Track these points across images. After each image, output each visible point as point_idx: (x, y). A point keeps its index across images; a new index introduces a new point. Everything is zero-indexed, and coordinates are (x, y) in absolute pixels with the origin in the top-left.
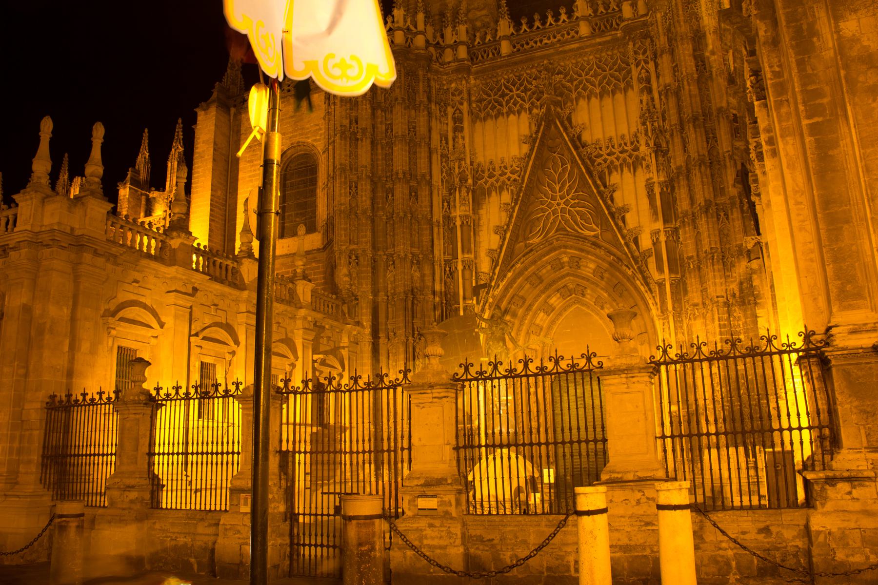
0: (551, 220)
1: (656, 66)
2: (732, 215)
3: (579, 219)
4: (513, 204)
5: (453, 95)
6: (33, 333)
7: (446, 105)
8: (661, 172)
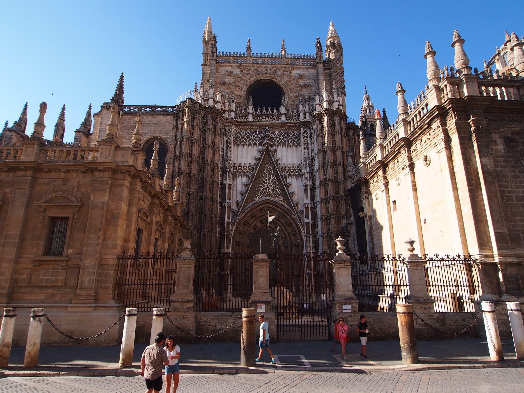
0: (264, 192)
4: (249, 183)
6: (108, 218)
7: (224, 136)
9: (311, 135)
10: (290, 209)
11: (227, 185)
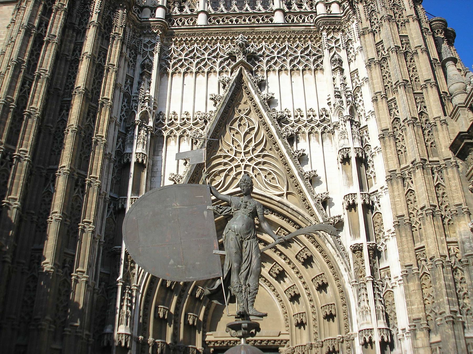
0: (233, 174)
2: (447, 174)
5: (145, 46)
9: (347, 43)
10: (307, 216)
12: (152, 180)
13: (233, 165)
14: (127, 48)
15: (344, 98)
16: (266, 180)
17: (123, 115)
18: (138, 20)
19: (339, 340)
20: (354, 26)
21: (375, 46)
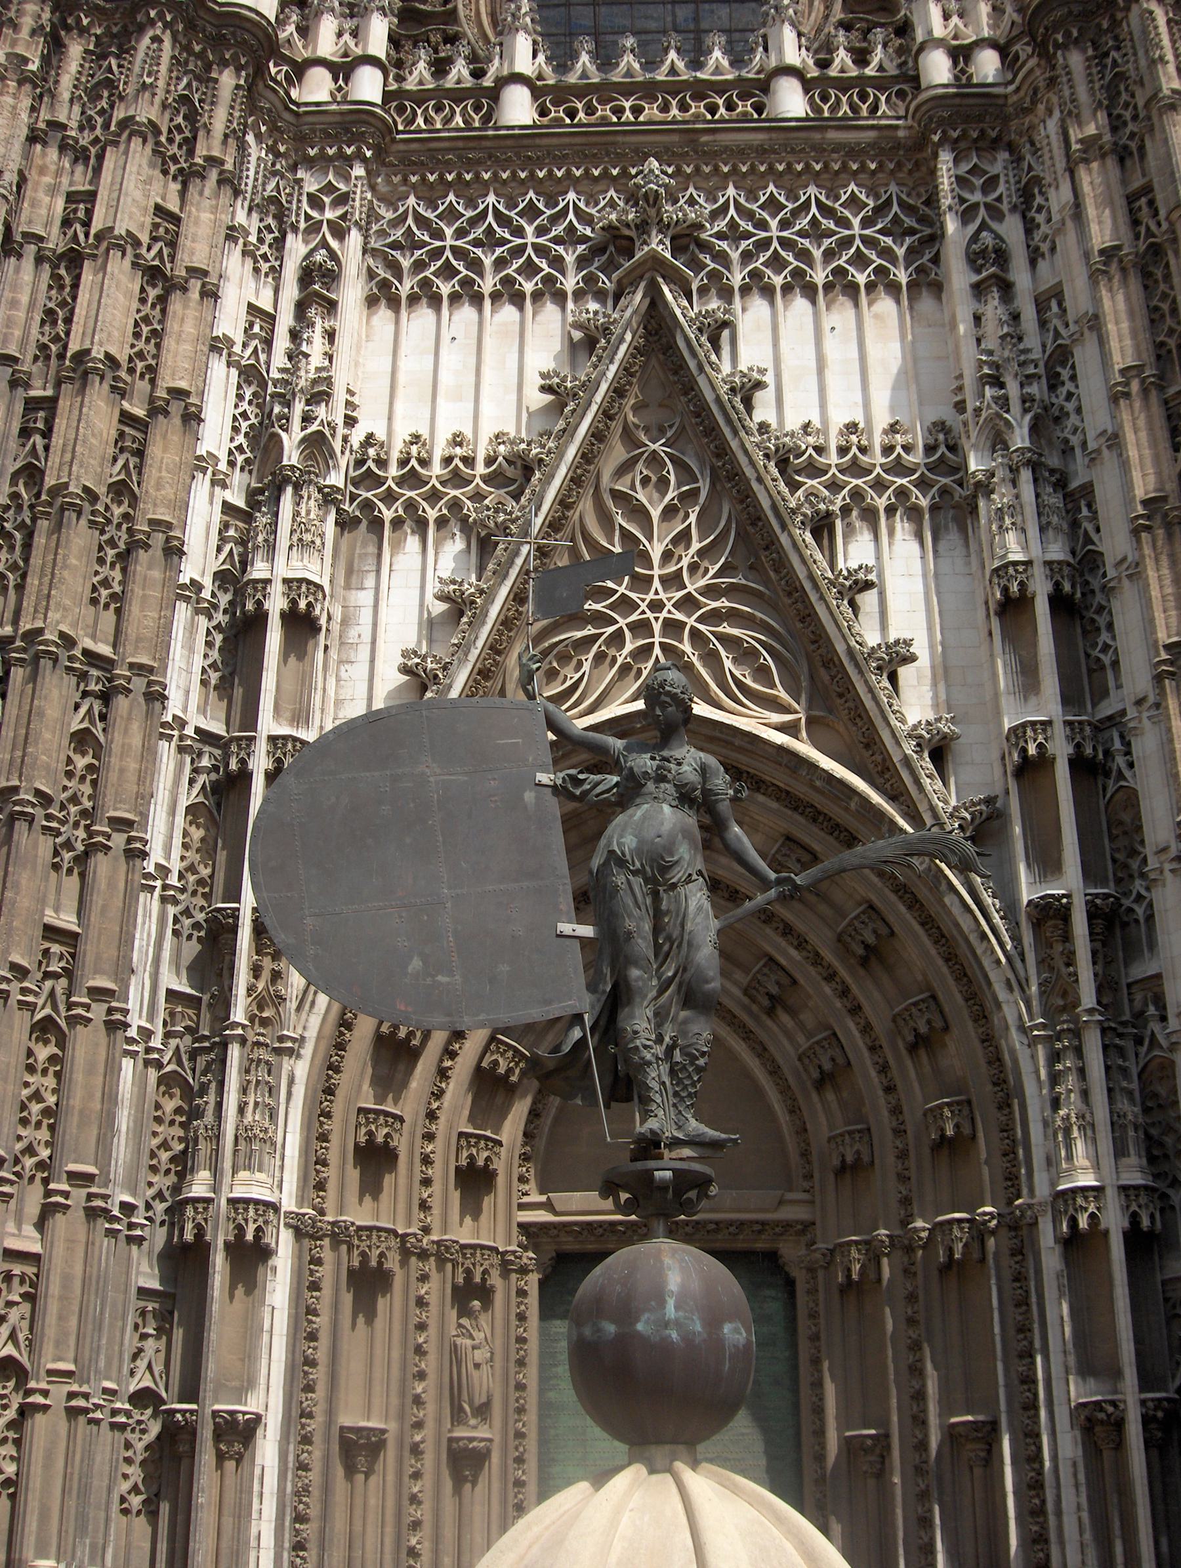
1: (1030, 228)
3: (728, 664)
8: (1051, 533)
10: (876, 798)
11: (277, 589)
12: (343, 675)
13: (622, 622)
14: (250, 210)
15: (1013, 389)
16: (737, 673)
17: (240, 448)
18: (287, 108)
19: (985, 1223)
20: (1052, 125)
21: (1124, 202)
